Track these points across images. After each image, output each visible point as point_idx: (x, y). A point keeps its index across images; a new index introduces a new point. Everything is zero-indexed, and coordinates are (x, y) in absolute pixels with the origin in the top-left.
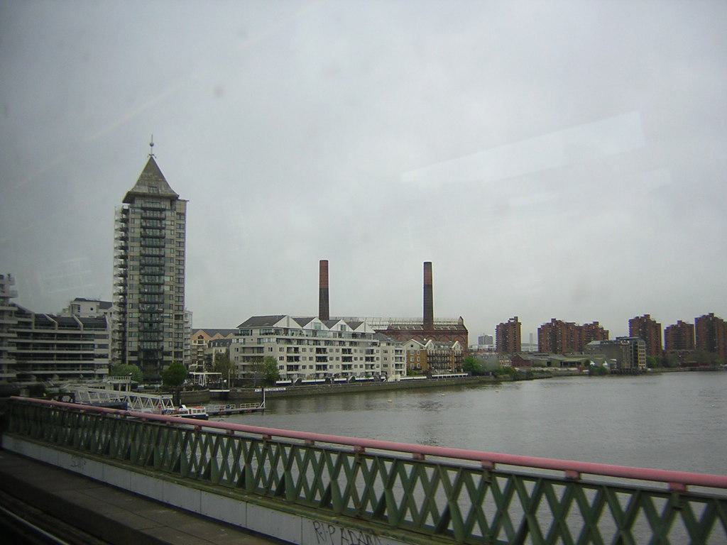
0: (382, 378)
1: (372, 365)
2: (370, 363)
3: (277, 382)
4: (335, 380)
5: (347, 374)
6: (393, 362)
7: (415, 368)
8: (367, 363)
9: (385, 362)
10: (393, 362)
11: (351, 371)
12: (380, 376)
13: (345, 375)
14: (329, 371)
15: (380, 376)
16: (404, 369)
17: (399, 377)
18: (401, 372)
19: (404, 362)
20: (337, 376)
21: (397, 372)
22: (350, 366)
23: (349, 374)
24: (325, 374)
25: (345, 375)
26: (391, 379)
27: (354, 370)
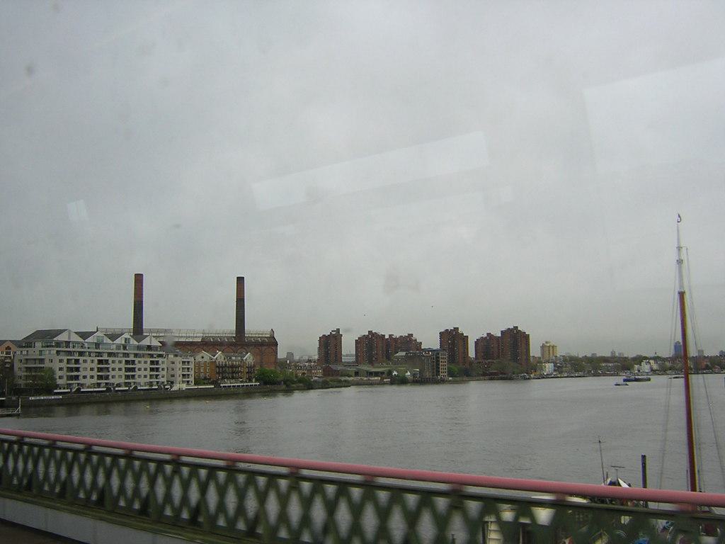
0: (166, 387)
1: (157, 376)
2: (155, 373)
3: (55, 391)
4: (116, 389)
5: (130, 383)
6: (180, 372)
7: (205, 378)
8: (152, 373)
9: (172, 373)
10: (180, 372)
11: (133, 381)
12: (164, 386)
13: (127, 384)
14: (111, 381)
15: (164, 386)
16: (192, 379)
17: (184, 387)
18: (188, 382)
19: (192, 373)
20: (119, 385)
21: (183, 382)
22: (133, 377)
23: (132, 384)
24: (106, 384)
25: (127, 384)
26: (175, 388)
27: (137, 380)
